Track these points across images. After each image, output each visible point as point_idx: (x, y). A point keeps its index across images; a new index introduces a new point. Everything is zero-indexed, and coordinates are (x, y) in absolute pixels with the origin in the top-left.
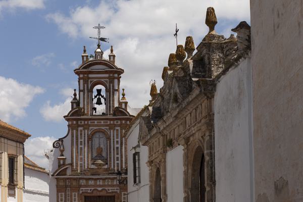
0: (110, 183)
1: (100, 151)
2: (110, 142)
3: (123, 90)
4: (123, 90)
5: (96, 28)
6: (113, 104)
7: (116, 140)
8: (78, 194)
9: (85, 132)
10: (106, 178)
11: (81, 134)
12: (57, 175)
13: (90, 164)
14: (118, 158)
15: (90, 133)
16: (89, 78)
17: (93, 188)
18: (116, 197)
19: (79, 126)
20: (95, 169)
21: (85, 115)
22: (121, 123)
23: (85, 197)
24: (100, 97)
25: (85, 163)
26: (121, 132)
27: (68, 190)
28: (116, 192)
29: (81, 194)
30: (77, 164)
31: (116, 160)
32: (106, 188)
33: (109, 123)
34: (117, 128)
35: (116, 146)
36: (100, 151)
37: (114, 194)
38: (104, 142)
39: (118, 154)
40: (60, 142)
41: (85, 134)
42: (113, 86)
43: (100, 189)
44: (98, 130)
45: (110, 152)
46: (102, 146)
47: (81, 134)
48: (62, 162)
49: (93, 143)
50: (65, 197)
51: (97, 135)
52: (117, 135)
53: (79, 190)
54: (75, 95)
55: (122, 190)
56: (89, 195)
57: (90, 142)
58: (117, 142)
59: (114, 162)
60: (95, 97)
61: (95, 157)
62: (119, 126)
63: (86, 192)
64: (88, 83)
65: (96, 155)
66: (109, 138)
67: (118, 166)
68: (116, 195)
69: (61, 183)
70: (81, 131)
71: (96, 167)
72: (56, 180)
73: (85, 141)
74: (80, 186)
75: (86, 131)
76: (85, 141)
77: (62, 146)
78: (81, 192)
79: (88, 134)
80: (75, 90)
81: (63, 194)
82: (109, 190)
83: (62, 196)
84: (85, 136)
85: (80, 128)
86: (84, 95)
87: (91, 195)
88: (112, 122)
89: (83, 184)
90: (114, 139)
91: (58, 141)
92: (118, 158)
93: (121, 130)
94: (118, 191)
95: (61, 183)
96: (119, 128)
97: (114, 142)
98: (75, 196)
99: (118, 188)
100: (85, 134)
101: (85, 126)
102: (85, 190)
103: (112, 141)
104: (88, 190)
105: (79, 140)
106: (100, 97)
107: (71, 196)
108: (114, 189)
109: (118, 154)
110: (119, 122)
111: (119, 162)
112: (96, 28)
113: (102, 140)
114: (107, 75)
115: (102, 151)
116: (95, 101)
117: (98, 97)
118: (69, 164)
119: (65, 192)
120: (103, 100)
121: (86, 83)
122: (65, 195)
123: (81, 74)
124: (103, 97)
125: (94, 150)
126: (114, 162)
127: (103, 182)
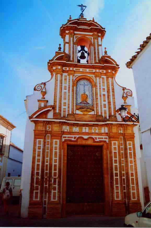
0: (97, 131)
1: (85, 97)
2: (96, 89)
3: (105, 48)
4: (105, 48)
5: (79, 6)
6: (98, 55)
7: (102, 87)
8: (60, 141)
9: (69, 77)
10: (94, 125)
11: (65, 79)
12: (36, 117)
13: (75, 109)
14: (105, 105)
15: (74, 79)
16: (75, 34)
17: (77, 136)
19: (64, 71)
20: (80, 115)
21: (71, 61)
22: (107, 72)
23: (68, 145)
24: (84, 52)
25: (69, 107)
26: (107, 80)
27: (48, 136)
28: (105, 141)
29: (63, 142)
30: (60, 107)
31: (103, 106)
32: (93, 137)
34: (102, 76)
35: (103, 93)
36: (85, 97)
37: (101, 144)
38: (89, 89)
40: (43, 86)
41: (69, 79)
42: (98, 42)
43: (86, 137)
44: (83, 77)
45: (97, 99)
46: (87, 93)
47: (65, 79)
48: (43, 105)
49: (78, 90)
50: (44, 146)
51: (82, 82)
52: (103, 82)
53: (61, 137)
54: (60, 48)
55: (111, 139)
58: (104, 89)
59: (101, 109)
60: (79, 51)
61: (81, 103)
62: (105, 74)
64: (74, 37)
66: (94, 85)
67: (105, 113)
68: (105, 145)
69: (40, 128)
70: (66, 76)
71: (82, 113)
72: (33, 124)
73: (69, 86)
74: (64, 133)
75: (71, 76)
76: (69, 86)
78: (63, 139)
79: (73, 80)
80: (60, 45)
81: (42, 140)
82: (96, 138)
83: (40, 142)
84: (69, 81)
85: (64, 74)
86: (70, 45)
87: (75, 143)
88: (98, 71)
89: (66, 131)
90: (100, 86)
92: (105, 105)
93: (107, 78)
94: (107, 140)
95: (40, 128)
96: (105, 77)
97: (100, 88)
98: (56, 144)
99: (107, 137)
100: (69, 79)
101: (69, 72)
102: (68, 137)
103: (98, 87)
104: (72, 138)
106: (84, 52)
107: (52, 143)
108: (102, 138)
109: (105, 101)
110: (105, 71)
111: (107, 109)
112: (79, 6)
113: (87, 88)
114: (92, 34)
116: (79, 54)
117: (81, 52)
118: (51, 106)
119: (45, 139)
120: (86, 55)
122: (45, 142)
123: (67, 30)
124: (86, 52)
125: (78, 97)
126: (101, 109)
127: (89, 129)
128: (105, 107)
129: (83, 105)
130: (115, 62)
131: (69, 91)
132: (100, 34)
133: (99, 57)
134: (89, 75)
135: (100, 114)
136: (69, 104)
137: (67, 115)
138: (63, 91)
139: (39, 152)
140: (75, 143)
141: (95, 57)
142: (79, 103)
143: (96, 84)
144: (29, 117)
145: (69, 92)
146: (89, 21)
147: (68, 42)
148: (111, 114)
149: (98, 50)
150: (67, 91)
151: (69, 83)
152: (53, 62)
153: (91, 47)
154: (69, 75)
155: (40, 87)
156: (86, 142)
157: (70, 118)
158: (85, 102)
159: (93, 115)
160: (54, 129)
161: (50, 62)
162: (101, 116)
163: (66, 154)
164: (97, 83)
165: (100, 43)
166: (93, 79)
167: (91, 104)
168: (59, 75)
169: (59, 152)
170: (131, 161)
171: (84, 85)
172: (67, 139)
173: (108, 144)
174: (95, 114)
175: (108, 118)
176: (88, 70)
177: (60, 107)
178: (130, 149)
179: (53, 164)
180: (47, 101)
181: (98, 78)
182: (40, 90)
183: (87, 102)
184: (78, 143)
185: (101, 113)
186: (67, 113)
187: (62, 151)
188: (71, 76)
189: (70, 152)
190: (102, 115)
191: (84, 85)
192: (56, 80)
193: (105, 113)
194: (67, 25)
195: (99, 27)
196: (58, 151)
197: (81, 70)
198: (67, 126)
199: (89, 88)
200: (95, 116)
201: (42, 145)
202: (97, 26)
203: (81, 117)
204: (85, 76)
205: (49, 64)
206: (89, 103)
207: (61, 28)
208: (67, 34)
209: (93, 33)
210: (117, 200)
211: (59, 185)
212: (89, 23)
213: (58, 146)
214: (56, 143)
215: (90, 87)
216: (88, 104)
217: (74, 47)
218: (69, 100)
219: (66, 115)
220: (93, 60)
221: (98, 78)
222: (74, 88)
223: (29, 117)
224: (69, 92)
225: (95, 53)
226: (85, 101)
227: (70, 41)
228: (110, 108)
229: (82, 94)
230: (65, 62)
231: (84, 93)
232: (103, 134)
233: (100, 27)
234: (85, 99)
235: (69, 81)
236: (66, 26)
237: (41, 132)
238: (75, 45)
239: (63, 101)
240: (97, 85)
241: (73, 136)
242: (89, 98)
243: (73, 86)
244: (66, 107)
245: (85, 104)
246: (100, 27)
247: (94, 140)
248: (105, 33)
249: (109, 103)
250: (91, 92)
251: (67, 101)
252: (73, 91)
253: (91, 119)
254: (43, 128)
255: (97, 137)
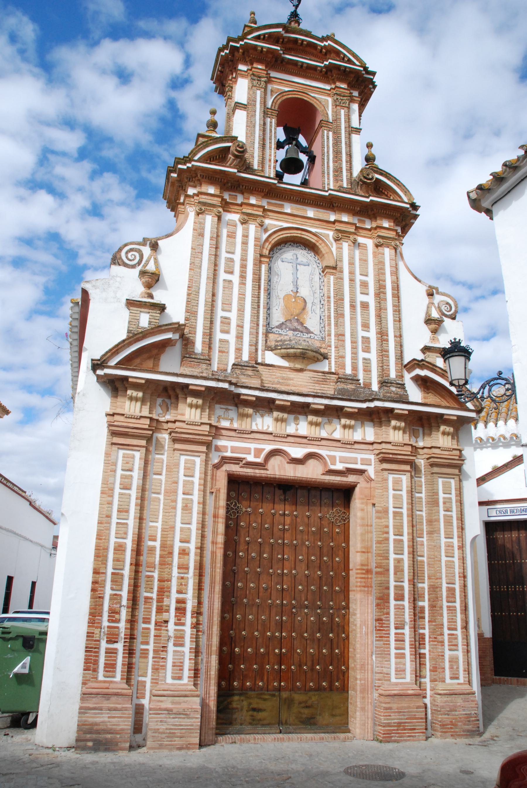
0: (338, 434)
7: (359, 278)
11: (232, 235)
12: (120, 365)
15: (265, 236)
17: (268, 448)
18: (357, 490)
19: (226, 206)
25: (239, 337)
28: (361, 472)
29: (217, 467)
30: (209, 335)
32: (323, 452)
33: (332, 218)
34: (360, 240)
35: (360, 298)
37: (351, 479)
39: (366, 326)
40: (147, 251)
41: (246, 236)
43: (298, 452)
45: (340, 315)
46: (304, 292)
52: (364, 261)
56: (249, 471)
57: (264, 267)
59: (355, 354)
61: (280, 326)
63: (237, 461)
65: (282, 320)
71: (284, 363)
73: (244, 259)
75: (252, 228)
76: (244, 259)
77: (152, 262)
79: (257, 239)
82: (333, 459)
84: (245, 243)
90: (352, 273)
91: (139, 244)
92: (366, 340)
93: (377, 246)
96: (369, 243)
97: (352, 280)
100: (246, 236)
104: (248, 451)
105: (224, 255)
107: (173, 468)
111: (373, 356)
113: (304, 272)
115: (304, 309)
121: (259, 88)
126: (355, 354)
128: (367, 350)
129: (290, 333)
130: (406, 191)
131: (243, 277)
132: (356, 94)
133: (350, 170)
134: (313, 230)
135: (349, 371)
136: (240, 326)
137: (234, 365)
138: (222, 276)
139: (125, 499)
140: (257, 471)
141: (338, 171)
142: (277, 327)
143: (338, 263)
144: (92, 360)
145: (243, 283)
146: (323, 39)
147: (246, 103)
148: (388, 375)
149: (349, 145)
150: (235, 278)
151: (245, 251)
152: (189, 165)
153: (326, 132)
154: (244, 222)
155: (137, 255)
156: (295, 470)
157: (244, 380)
158: (296, 324)
159: (323, 373)
160: (183, 415)
161: (180, 166)
162: (354, 380)
163: (222, 512)
164: (341, 261)
165: (355, 123)
166: (327, 245)
167: (318, 333)
168: (209, 220)
169: (199, 503)
170: (449, 546)
171: (296, 265)
172: (229, 454)
173: (371, 480)
174: (333, 370)
175: (375, 387)
176: (311, 213)
177: (209, 335)
178: (448, 505)
179: (177, 545)
180: (162, 308)
181: (345, 246)
182: (133, 267)
183: (302, 324)
184: (268, 472)
185: (355, 368)
186: (232, 360)
187: (211, 500)
188: (252, 228)
189: (235, 505)
190: (356, 375)
191: (296, 265)
192: (199, 233)
193: (367, 370)
194: (246, 41)
195: (354, 64)
196: (196, 497)
197: (288, 208)
198: (230, 407)
199: (312, 274)
200: (334, 377)
201: (136, 475)
202: (349, 61)
203: (283, 378)
204: (299, 232)
205: (174, 175)
206: (312, 329)
207: (220, 50)
208: (243, 76)
209: (335, 83)
210: (397, 684)
211: (196, 626)
212: (322, 48)
213: (196, 480)
214: (189, 469)
215: (318, 271)
216: (308, 331)
217: (264, 124)
218: (241, 310)
219: (227, 365)
220: (328, 177)
221: (345, 246)
222: (260, 270)
223: (92, 360)
224: (243, 283)
225: (337, 153)
226: (298, 320)
227: (252, 101)
228: (383, 353)
229: (287, 297)
230: (236, 171)
231: (295, 290)
232: (356, 446)
233: (357, 63)
234: (297, 315)
235: (245, 243)
236: (241, 43)
237: (133, 423)
238: (268, 120)
239: (220, 313)
240: (342, 268)
241: (252, 446)
242: (313, 311)
243: (258, 263)
244: (231, 338)
245: (295, 330)
246: (357, 63)
247: (325, 464)
248: (373, 92)
249: (382, 335)
250: (318, 291)
251: (233, 315)
252: (257, 280)
253: (318, 389)
254: (141, 408)
255: (338, 454)
